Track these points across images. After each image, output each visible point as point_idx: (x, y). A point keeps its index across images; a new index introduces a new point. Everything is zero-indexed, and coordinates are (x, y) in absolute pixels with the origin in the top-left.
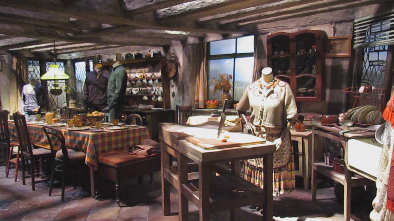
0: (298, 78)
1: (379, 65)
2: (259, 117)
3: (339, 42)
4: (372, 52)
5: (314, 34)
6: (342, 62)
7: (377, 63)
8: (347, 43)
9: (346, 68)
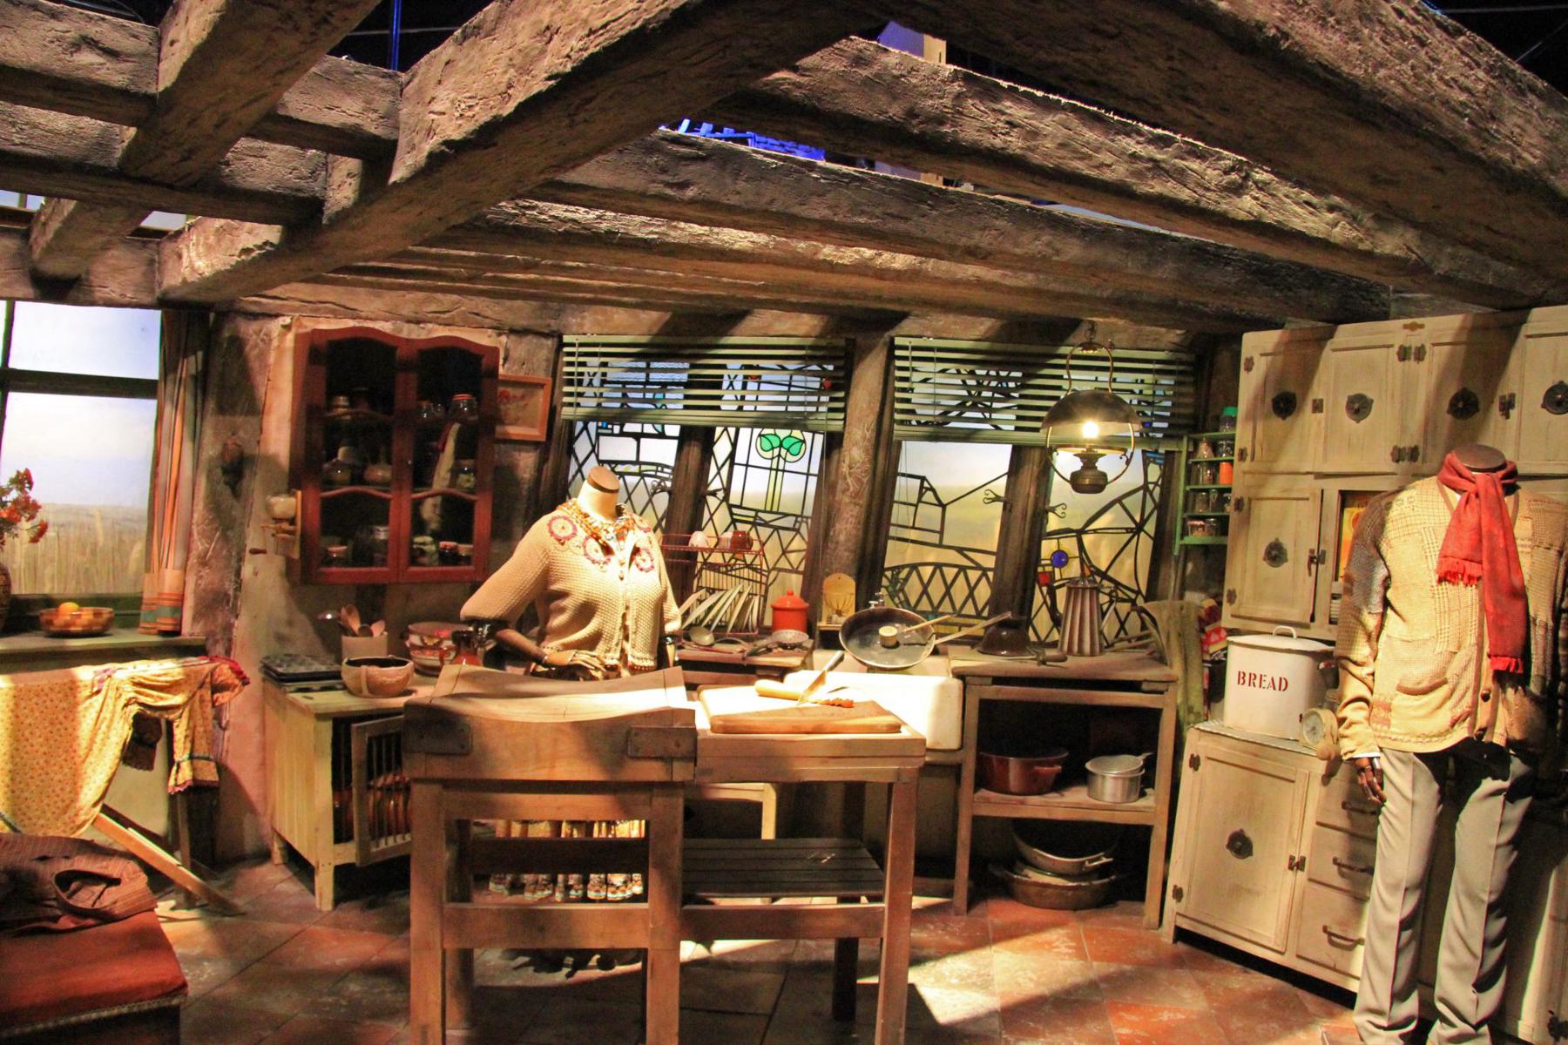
0: (324, 500)
1: (642, 475)
2: (618, 635)
3: (518, 392)
4: (612, 435)
5: (395, 349)
6: (516, 454)
7: (635, 469)
8: (540, 400)
9: (527, 476)
